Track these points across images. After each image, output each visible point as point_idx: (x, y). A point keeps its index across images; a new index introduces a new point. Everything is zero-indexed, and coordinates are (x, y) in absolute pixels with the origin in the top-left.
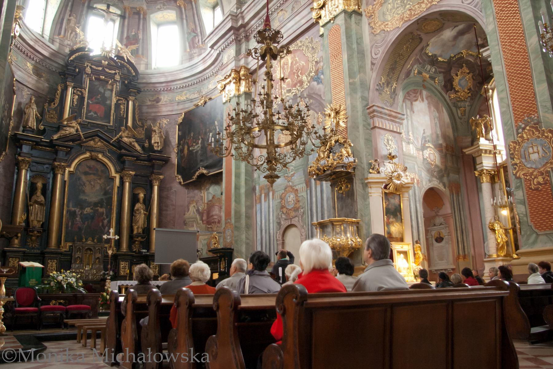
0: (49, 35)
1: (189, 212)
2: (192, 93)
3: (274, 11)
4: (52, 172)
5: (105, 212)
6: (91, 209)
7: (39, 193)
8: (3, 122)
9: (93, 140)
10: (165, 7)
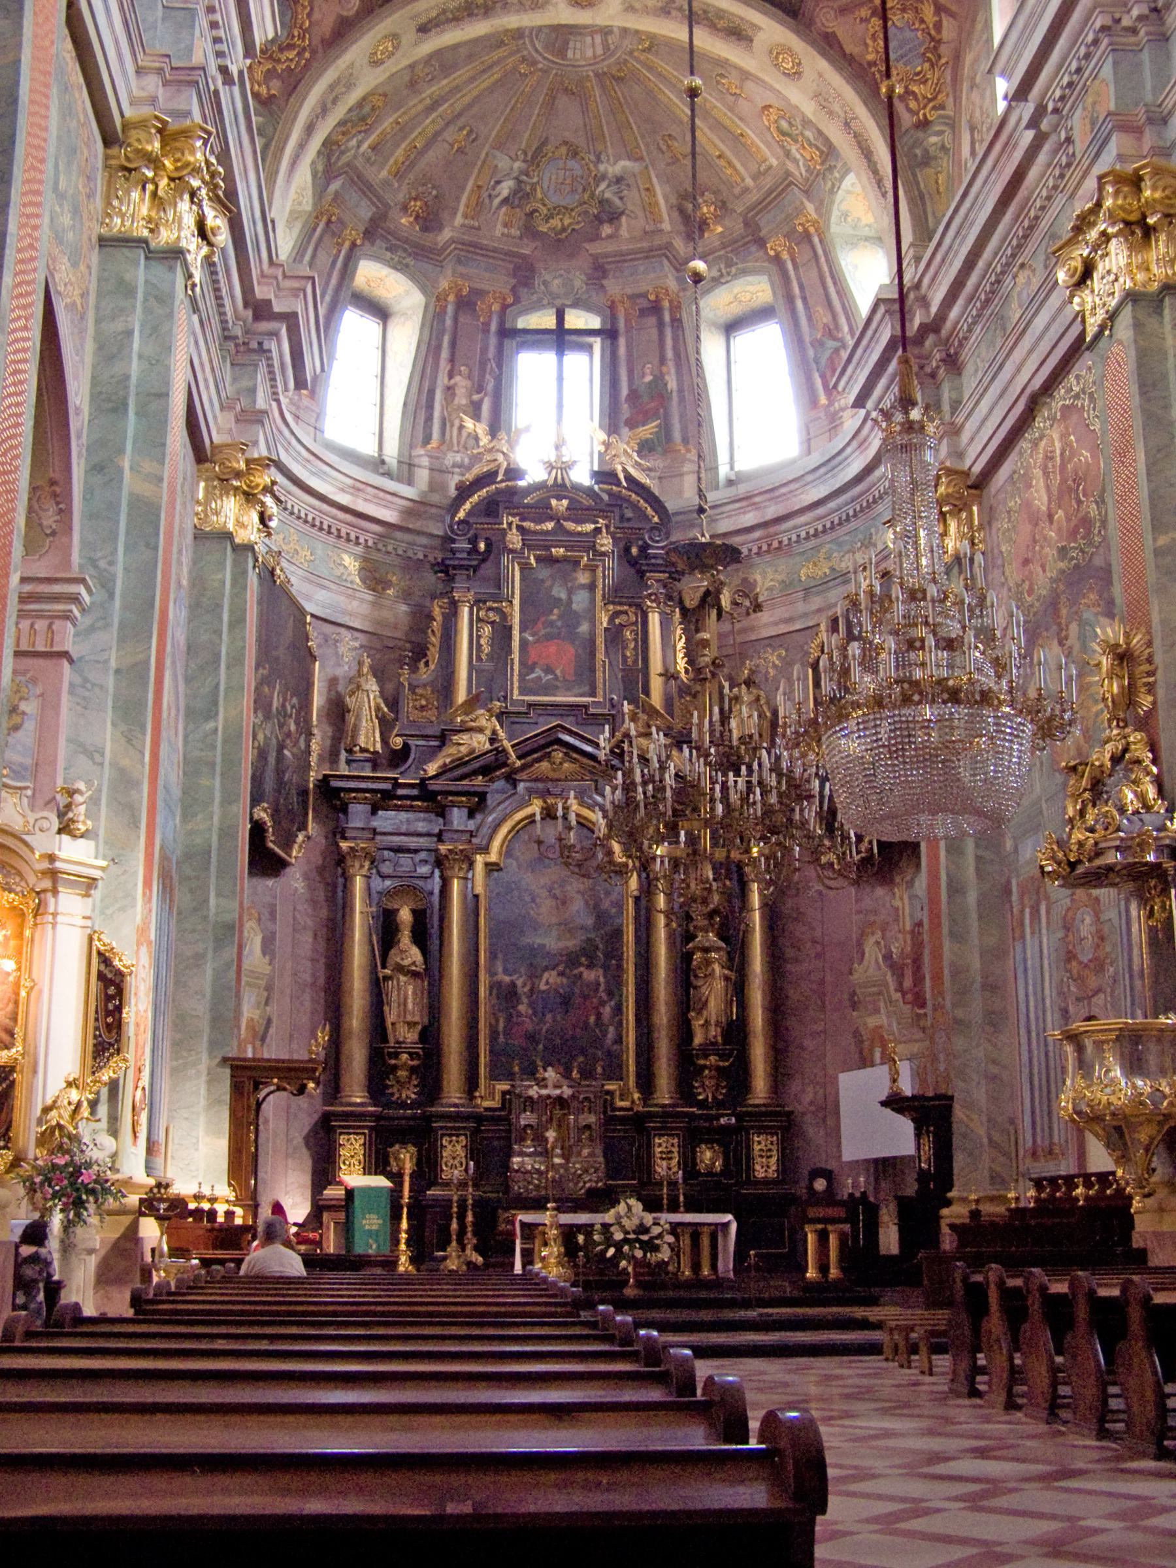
0: (395, 454)
1: (865, 962)
2: (848, 547)
3: (1003, 273)
4: (437, 873)
5: (602, 979)
6: (561, 974)
7: (405, 938)
8: (286, 752)
9: (548, 756)
10: (734, 270)
